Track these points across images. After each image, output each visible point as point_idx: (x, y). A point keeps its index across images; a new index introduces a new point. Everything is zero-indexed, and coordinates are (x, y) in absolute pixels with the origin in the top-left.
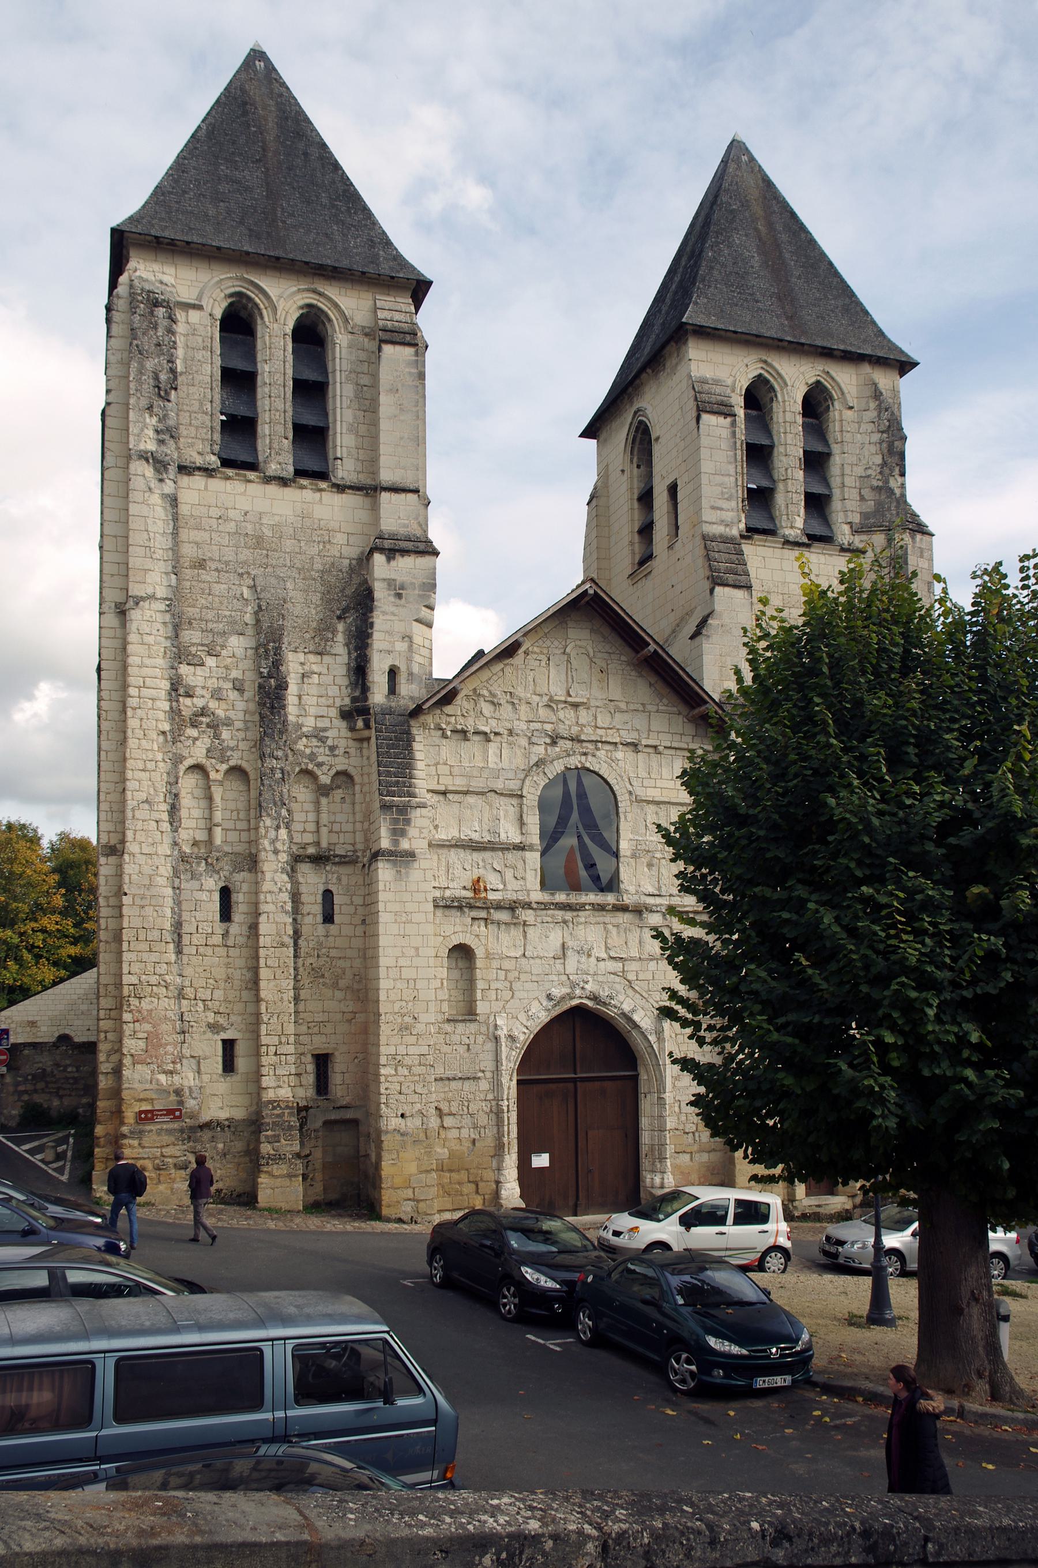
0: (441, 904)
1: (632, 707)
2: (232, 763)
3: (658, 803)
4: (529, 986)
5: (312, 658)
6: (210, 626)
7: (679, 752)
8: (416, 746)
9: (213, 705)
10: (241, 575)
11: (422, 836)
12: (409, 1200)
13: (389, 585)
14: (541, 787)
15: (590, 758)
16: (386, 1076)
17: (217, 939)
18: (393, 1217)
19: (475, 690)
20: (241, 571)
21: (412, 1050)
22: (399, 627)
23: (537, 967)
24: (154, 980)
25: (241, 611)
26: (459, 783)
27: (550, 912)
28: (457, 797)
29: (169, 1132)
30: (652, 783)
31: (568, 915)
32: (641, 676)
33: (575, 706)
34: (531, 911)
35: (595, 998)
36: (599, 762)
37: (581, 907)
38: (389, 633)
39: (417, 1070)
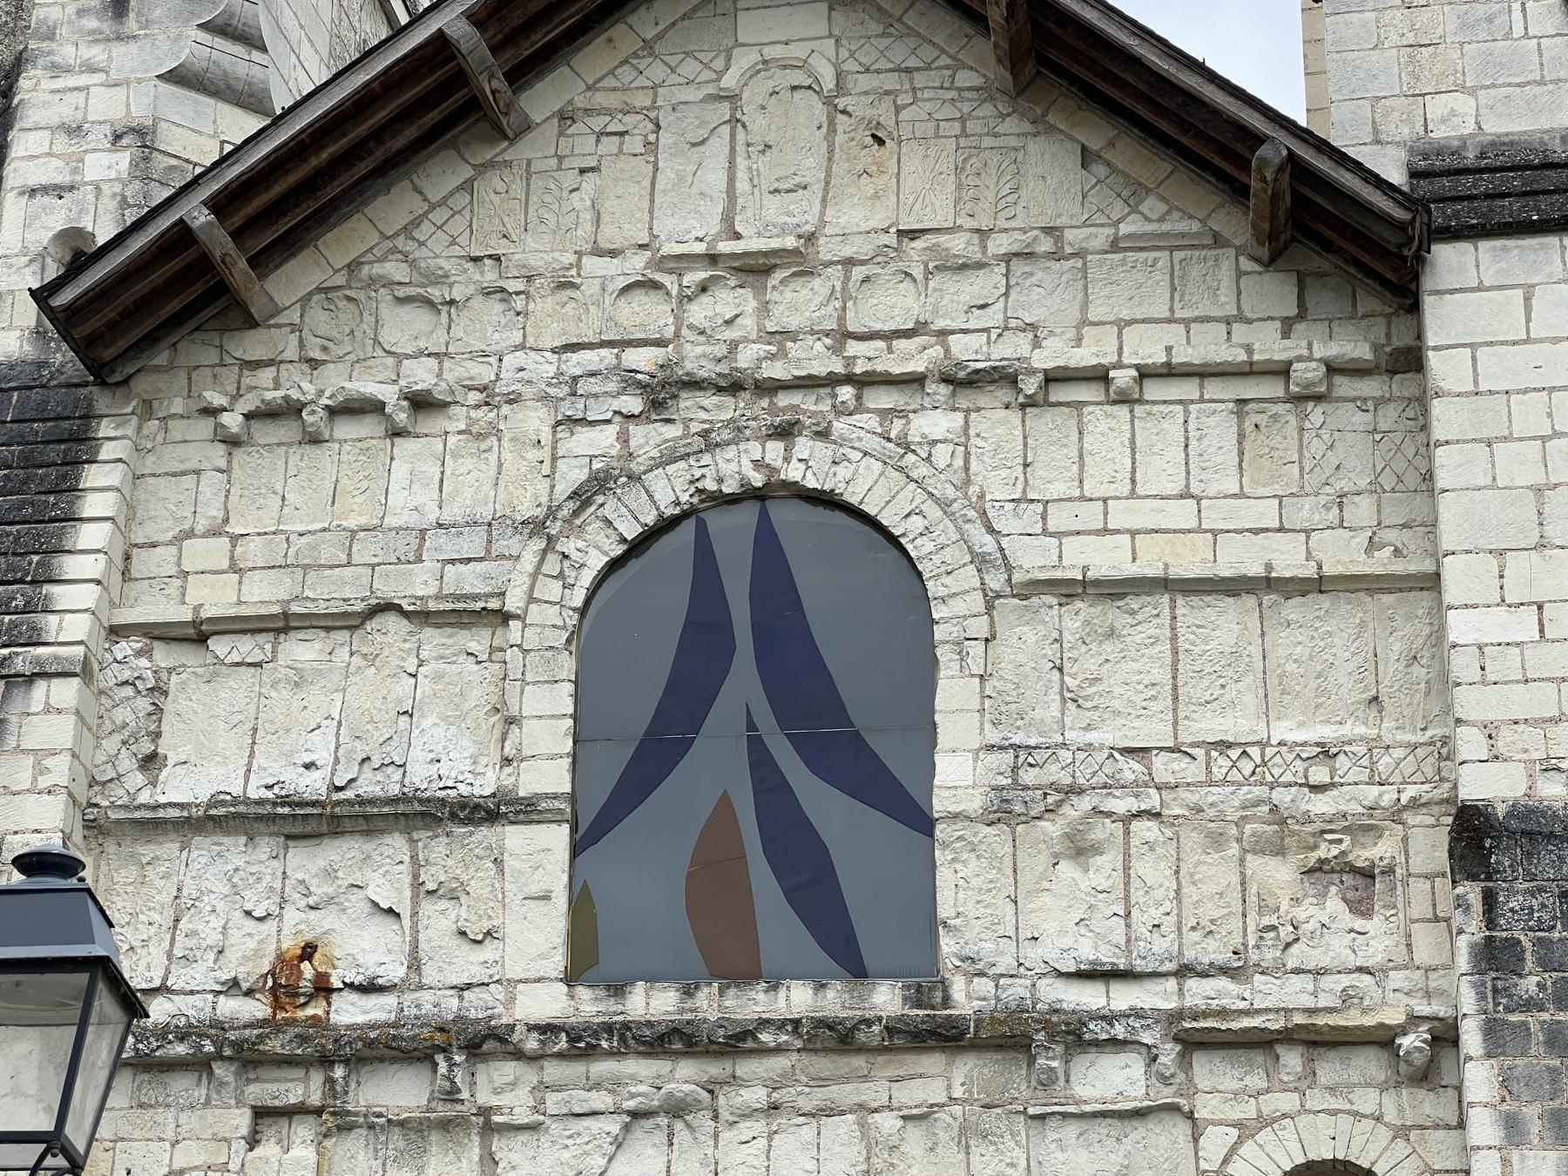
11: (44, 782)
28: (247, 647)
31: (684, 1076)
34: (508, 1070)
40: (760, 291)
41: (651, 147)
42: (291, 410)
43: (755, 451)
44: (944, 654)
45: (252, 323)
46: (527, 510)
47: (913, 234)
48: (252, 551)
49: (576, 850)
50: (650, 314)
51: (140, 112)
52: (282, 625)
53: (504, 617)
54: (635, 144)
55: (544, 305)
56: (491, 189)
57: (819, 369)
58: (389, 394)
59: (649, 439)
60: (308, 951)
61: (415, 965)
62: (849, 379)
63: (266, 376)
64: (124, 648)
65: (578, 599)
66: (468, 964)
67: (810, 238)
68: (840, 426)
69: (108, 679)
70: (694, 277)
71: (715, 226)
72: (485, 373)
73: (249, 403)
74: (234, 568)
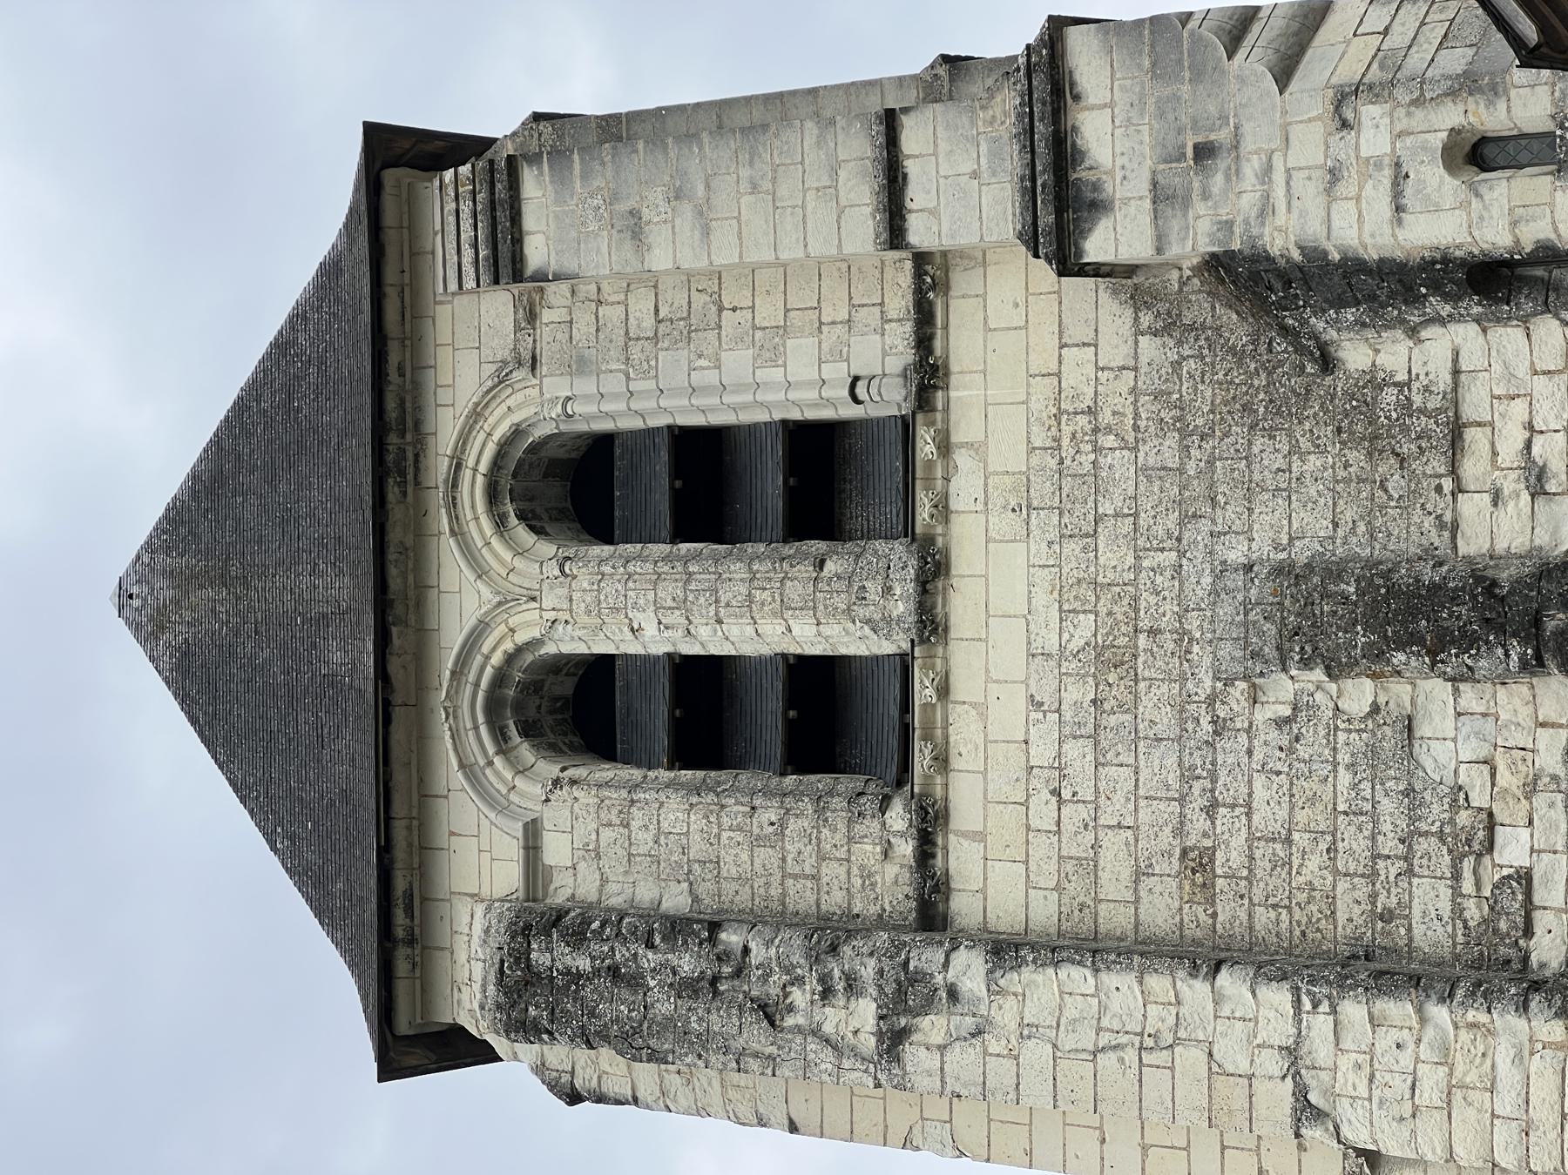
10: (1220, 727)
20: (1206, 726)
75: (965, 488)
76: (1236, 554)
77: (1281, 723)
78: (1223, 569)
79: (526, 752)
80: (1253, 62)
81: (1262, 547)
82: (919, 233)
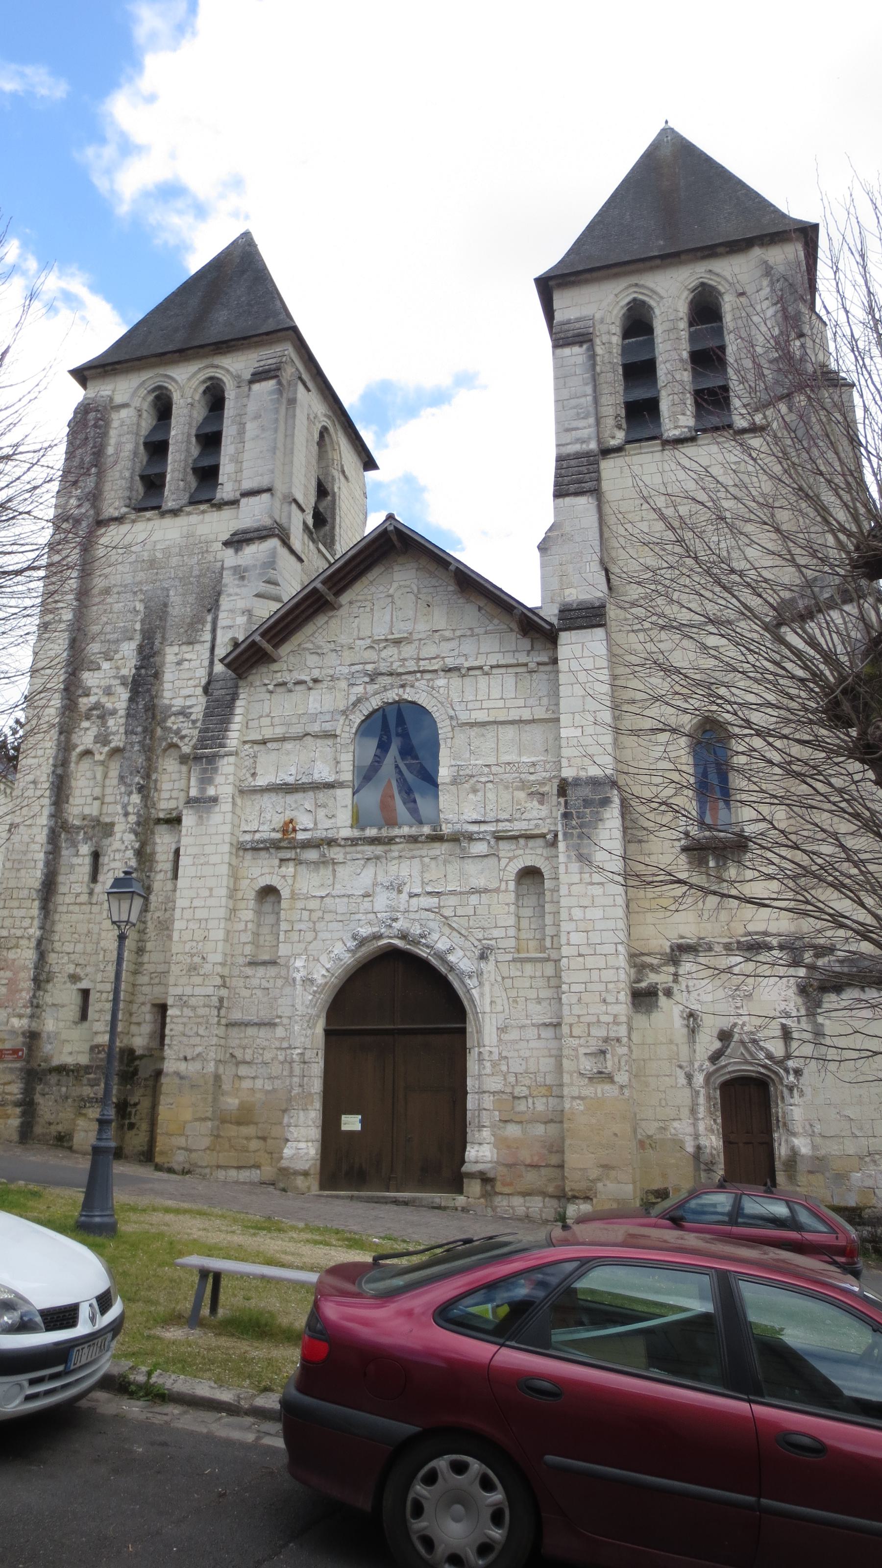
0: (248, 847)
1: (458, 633)
2: (113, 745)
3: (484, 724)
4: (334, 926)
5: (185, 648)
6: (108, 637)
7: (510, 670)
8: (239, 703)
9: (104, 700)
10: (135, 593)
12: (183, 1148)
13: (235, 571)
14: (356, 725)
15: (408, 689)
16: (172, 1017)
17: (84, 898)
18: (166, 1165)
19: (299, 645)
21: (198, 991)
22: (241, 604)
23: (341, 906)
24: (19, 933)
25: (132, 621)
26: (279, 731)
27: (359, 848)
28: (274, 745)
29: (11, 1070)
30: (478, 705)
31: (379, 850)
32: (468, 601)
33: (397, 642)
34: (338, 849)
35: (404, 937)
36: (418, 694)
37: (390, 841)
38: (232, 611)
39: (201, 1011)
40: (399, 648)
41: (372, 610)
42: (284, 684)
43: (396, 690)
44: (441, 742)
45: (275, 661)
46: (342, 708)
47: (436, 631)
48: (276, 721)
49: (354, 794)
50: (371, 655)
51: (249, 606)
52: (284, 739)
53: (336, 736)
54: (368, 609)
55: (346, 653)
56: (334, 624)
57: (411, 669)
58: (307, 679)
59: (371, 688)
60: (291, 821)
61: (316, 824)
62: (419, 672)
63: (279, 675)
64: (247, 746)
65: (354, 730)
66: (328, 824)
67: (411, 634)
68: (417, 684)
69: (243, 754)
70: (383, 645)
71: (387, 631)
72: (331, 672)
73: (274, 683)
74: (272, 725)
75: (194, 519)
76: (172, 593)
77: (135, 608)
78: (168, 590)
79: (151, 398)
80: (263, 587)
81: (172, 599)
82: (244, 501)
